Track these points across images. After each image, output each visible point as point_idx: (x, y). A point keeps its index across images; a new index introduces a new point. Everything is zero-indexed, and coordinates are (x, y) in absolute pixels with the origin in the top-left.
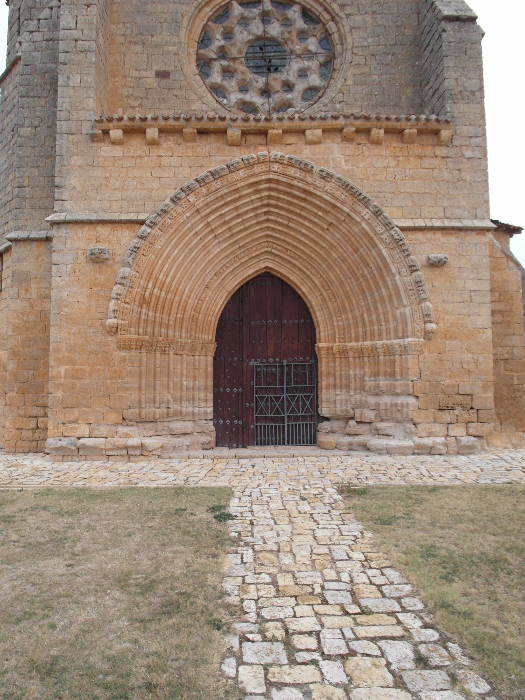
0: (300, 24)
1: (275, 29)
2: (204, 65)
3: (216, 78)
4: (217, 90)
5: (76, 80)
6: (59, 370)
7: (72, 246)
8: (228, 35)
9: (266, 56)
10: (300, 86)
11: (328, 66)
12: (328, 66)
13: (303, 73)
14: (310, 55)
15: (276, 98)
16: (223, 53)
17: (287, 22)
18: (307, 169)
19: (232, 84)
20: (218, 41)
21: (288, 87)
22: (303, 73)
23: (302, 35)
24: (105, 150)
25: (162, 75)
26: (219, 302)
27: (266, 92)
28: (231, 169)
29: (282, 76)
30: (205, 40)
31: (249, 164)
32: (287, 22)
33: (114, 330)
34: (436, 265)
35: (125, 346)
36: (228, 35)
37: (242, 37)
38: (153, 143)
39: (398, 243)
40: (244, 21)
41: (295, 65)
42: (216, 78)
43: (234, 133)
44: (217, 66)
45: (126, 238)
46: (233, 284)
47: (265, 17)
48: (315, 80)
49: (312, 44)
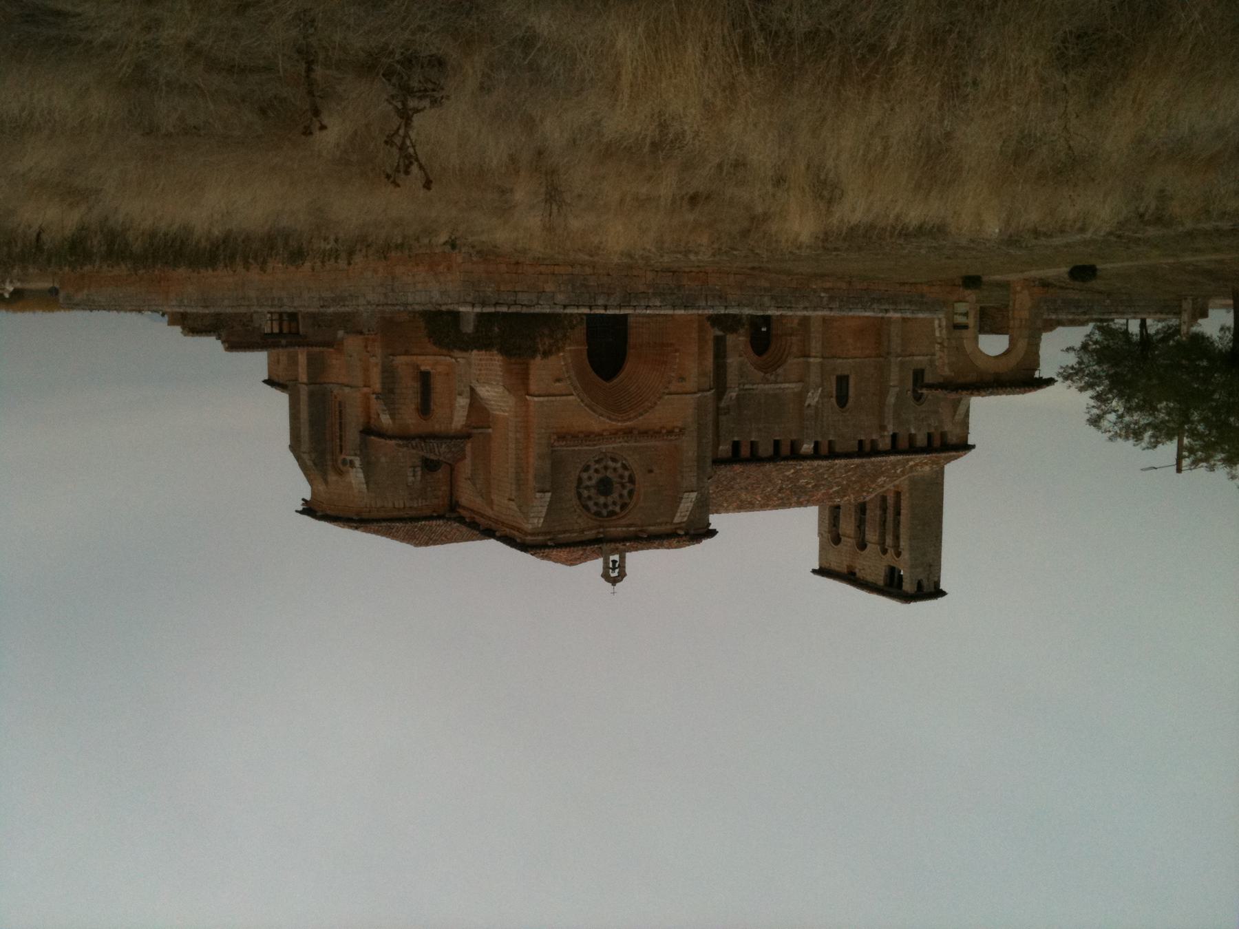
0: (590, 504)
1: (602, 500)
2: (632, 480)
3: (627, 474)
4: (625, 467)
5: (690, 454)
6: (694, 335)
7: (691, 384)
8: (621, 496)
9: (605, 486)
10: (592, 471)
11: (580, 480)
12: (580, 480)
13: (590, 478)
14: (587, 488)
15: (602, 465)
16: (623, 486)
17: (596, 504)
18: (609, 418)
19: (620, 471)
20: (625, 492)
21: (596, 471)
22: (590, 478)
23: (590, 498)
24: (680, 424)
25: (651, 471)
26: (628, 366)
27: (606, 468)
28: (636, 417)
29: (600, 476)
30: (631, 493)
31: (629, 419)
32: (596, 504)
33: (677, 351)
34: (558, 380)
35: (672, 344)
36: (621, 496)
37: (615, 495)
38: (663, 427)
39: (575, 388)
40: (614, 503)
41: (593, 482)
42: (627, 474)
43: (636, 432)
44: (626, 480)
45: (672, 388)
46: (622, 375)
47: (606, 506)
48: (585, 476)
49: (585, 493)
